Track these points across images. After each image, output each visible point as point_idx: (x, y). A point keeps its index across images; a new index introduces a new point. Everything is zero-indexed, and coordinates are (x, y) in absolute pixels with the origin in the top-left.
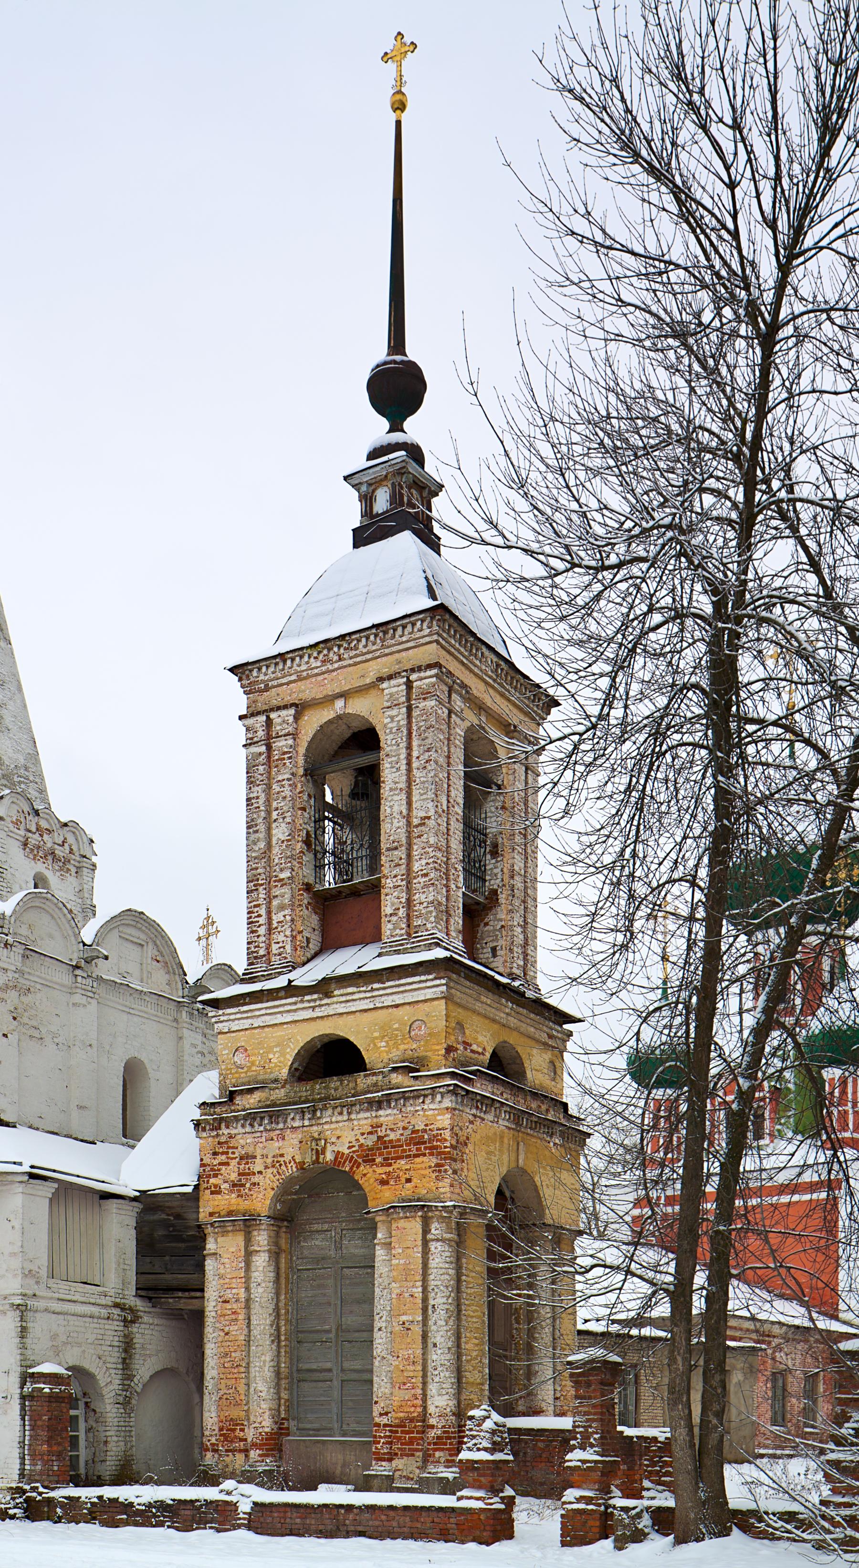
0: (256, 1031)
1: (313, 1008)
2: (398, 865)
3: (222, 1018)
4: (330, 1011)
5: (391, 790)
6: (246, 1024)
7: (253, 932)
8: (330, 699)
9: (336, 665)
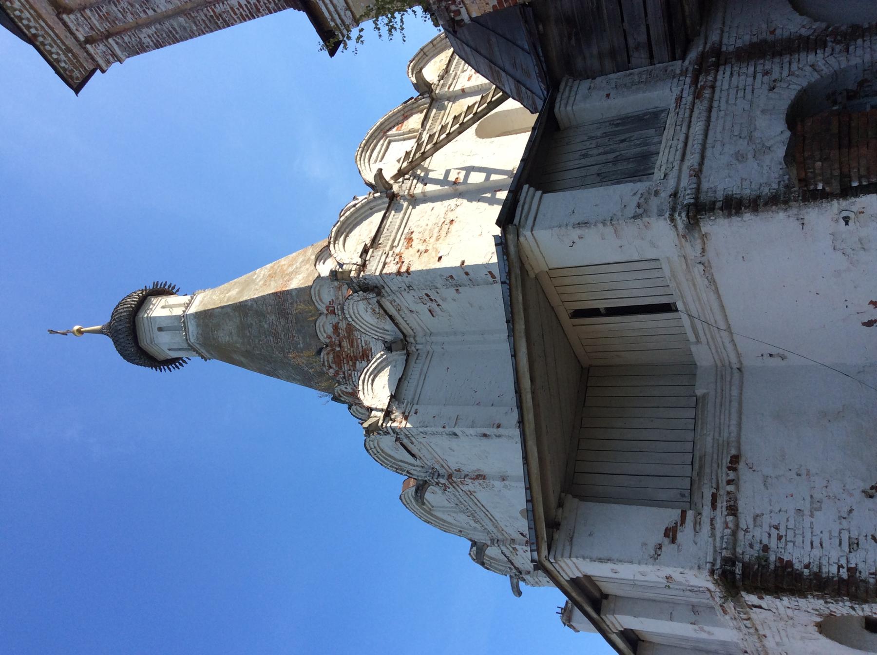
7: (258, 10)
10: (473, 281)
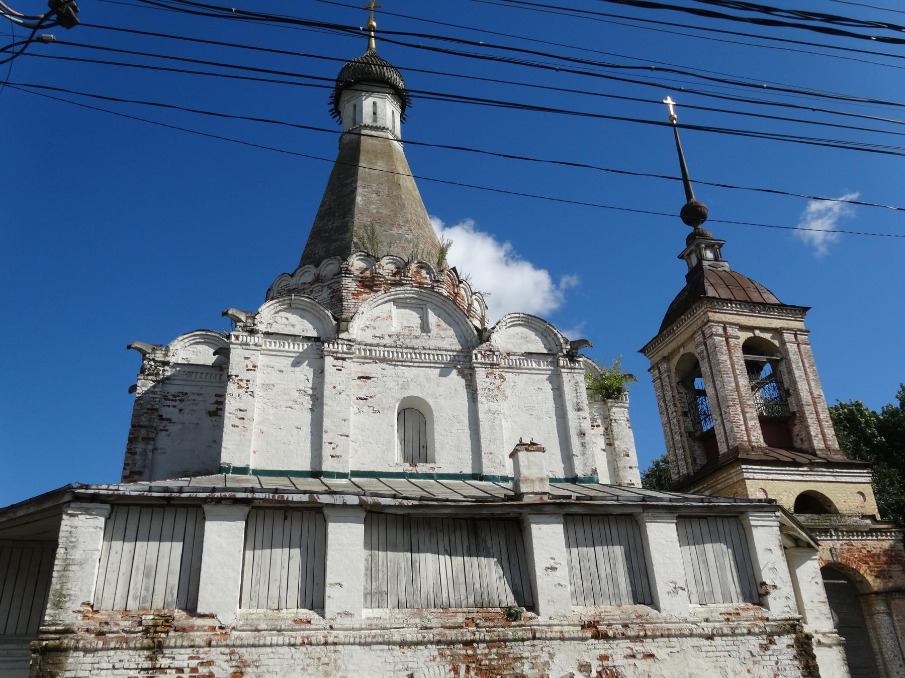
0: (770, 481)
1: (802, 475)
2: (811, 413)
3: (750, 471)
4: (812, 478)
5: (798, 377)
6: (764, 476)
8: (751, 329)
9: (757, 315)
10: (624, 469)
